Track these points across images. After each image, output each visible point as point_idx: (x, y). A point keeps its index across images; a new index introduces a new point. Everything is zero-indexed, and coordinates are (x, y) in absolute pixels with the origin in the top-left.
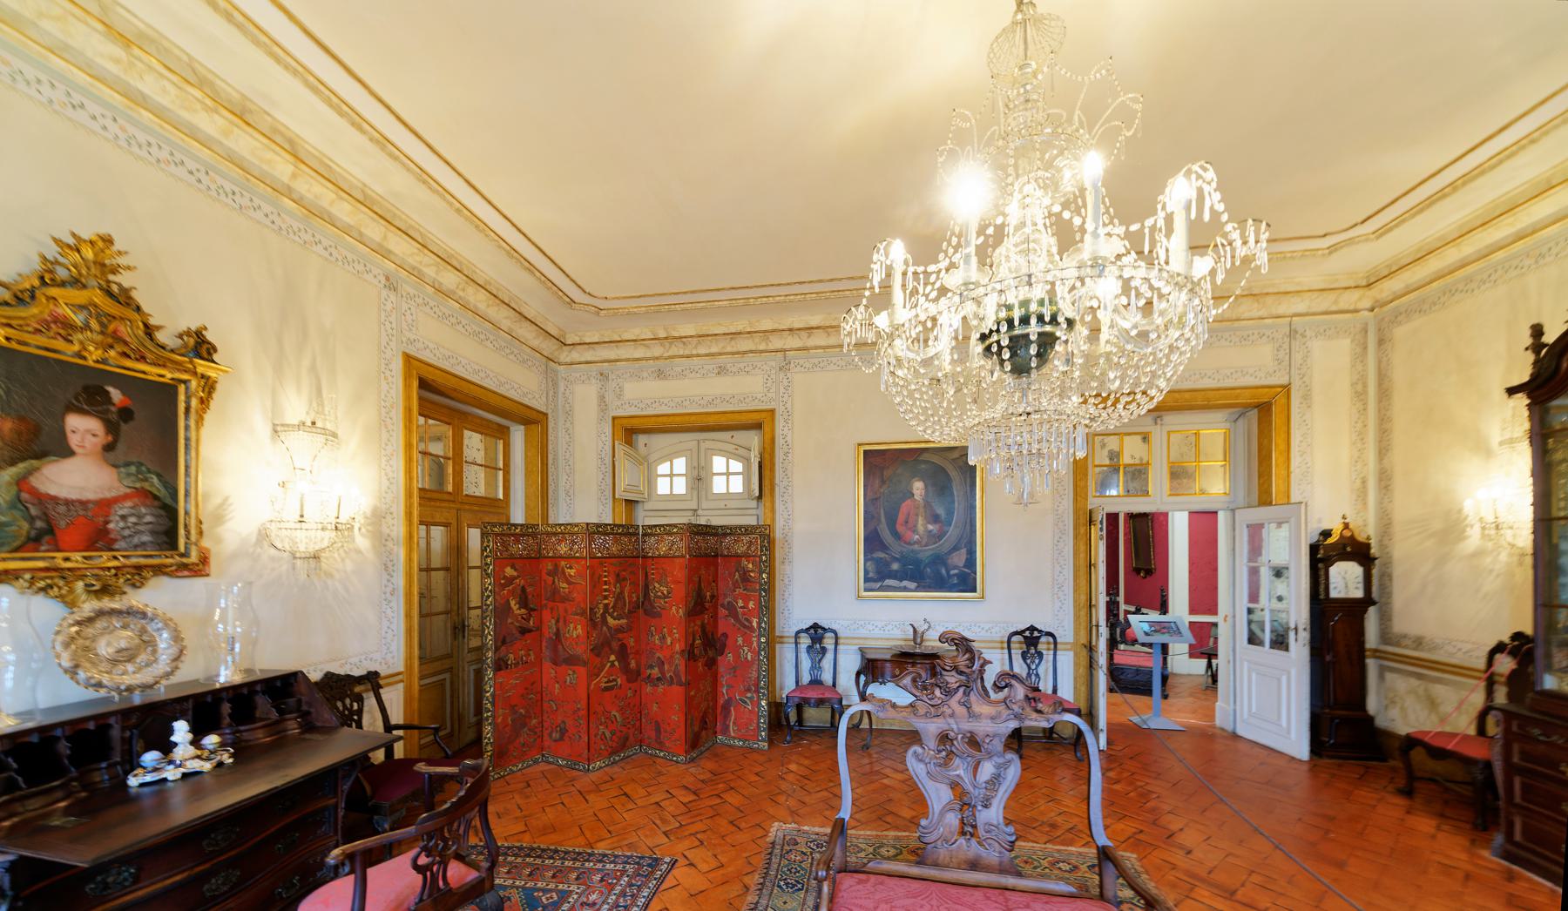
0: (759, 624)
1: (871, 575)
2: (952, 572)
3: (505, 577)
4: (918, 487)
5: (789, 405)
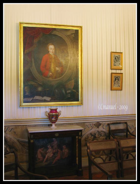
1: (27, 94)
2: (68, 92)
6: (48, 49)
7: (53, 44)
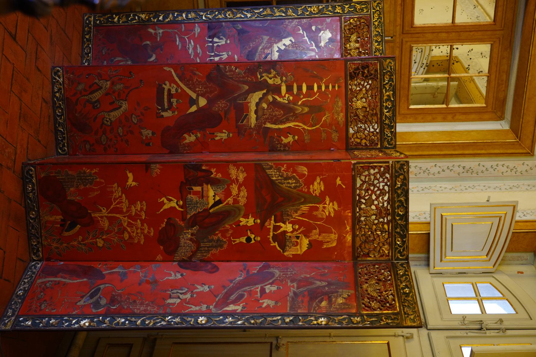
0: (232, 314)
3: (318, 30)
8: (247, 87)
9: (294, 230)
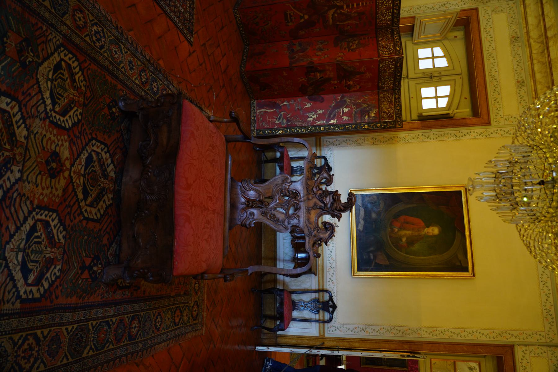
2: (371, 255)
4: (435, 231)
5: (494, 135)
6: (433, 226)
7: (440, 232)
8: (327, 8)
9: (353, 83)
